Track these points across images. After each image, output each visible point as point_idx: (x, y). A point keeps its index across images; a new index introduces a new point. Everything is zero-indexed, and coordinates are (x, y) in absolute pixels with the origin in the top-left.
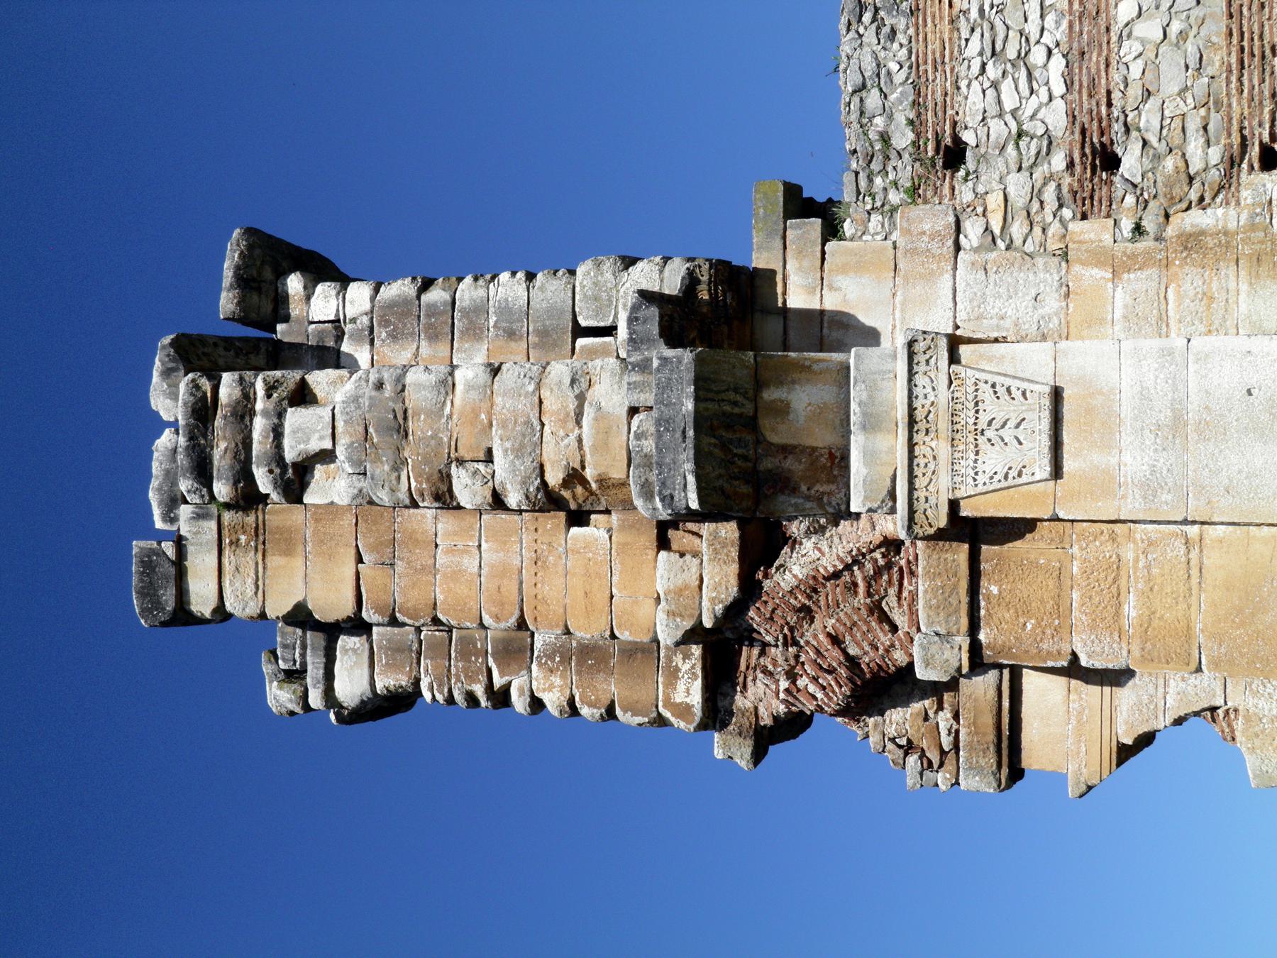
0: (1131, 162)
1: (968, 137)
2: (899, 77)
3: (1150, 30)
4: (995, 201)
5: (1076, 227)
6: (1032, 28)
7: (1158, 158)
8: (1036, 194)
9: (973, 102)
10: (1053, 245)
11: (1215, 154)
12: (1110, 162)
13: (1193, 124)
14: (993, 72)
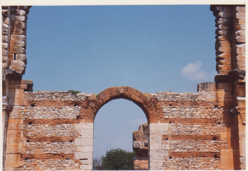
0: (29, 126)
1: (35, 107)
2: (43, 99)
3: (44, 128)
4: (27, 110)
5: (23, 120)
6: (46, 115)
7: (29, 129)
8: (27, 115)
9: (39, 108)
10: (21, 117)
11: (29, 135)
12: (30, 124)
13: (33, 133)
14: (42, 110)
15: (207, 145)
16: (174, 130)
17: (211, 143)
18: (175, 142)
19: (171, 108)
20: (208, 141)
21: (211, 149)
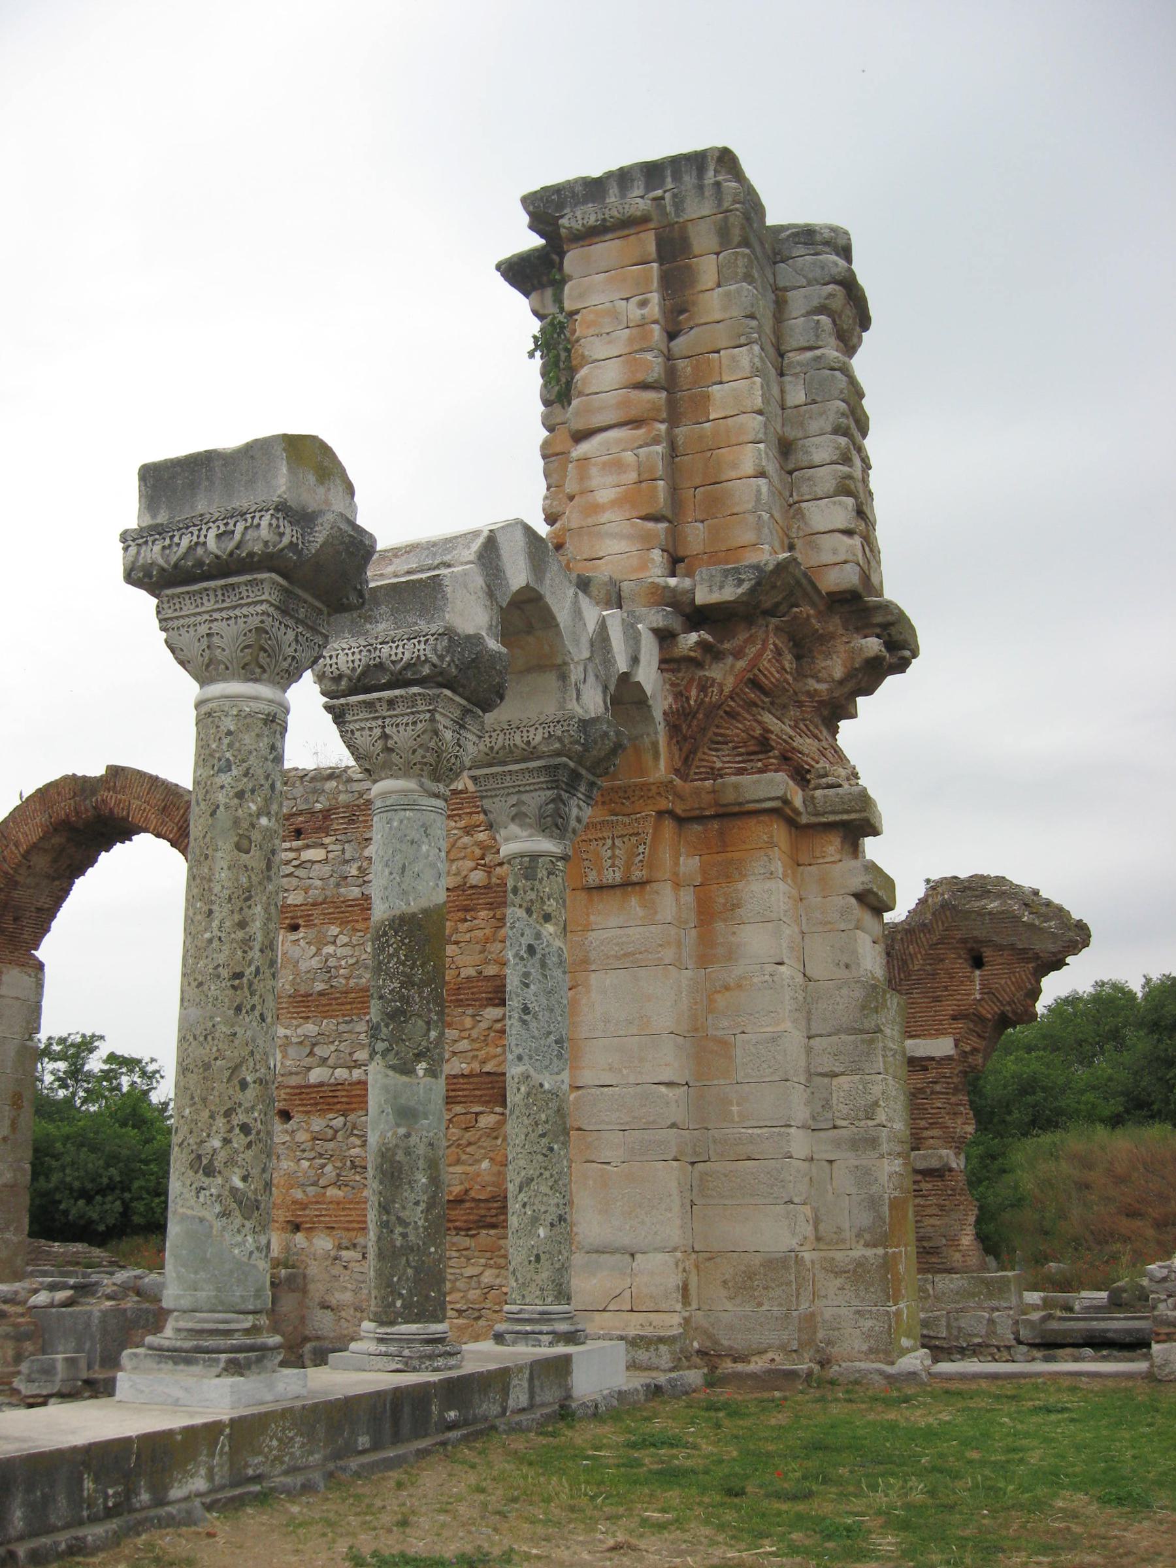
15: (465, 1034)
16: (304, 966)
17: (484, 1025)
18: (310, 1028)
19: (298, 850)
20: (470, 1011)
21: (482, 1054)
